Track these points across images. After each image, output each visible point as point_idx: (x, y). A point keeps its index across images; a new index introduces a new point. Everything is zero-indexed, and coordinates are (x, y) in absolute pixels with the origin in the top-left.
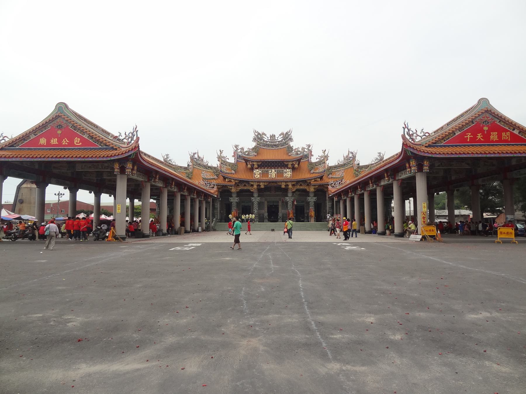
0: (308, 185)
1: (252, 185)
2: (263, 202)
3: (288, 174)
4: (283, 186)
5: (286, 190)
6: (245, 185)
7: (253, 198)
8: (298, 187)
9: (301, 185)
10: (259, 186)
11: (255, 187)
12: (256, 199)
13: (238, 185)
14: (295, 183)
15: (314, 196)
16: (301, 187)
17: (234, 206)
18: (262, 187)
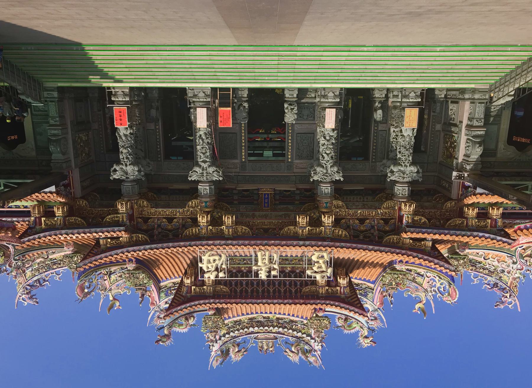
0: (146, 220)
1: (337, 222)
2: (300, 157)
3: (213, 262)
4: (228, 220)
5: (225, 197)
6: (362, 221)
7: (337, 177)
8: (178, 213)
9: (170, 220)
10: (316, 222)
11: (327, 220)
12: (326, 172)
13: (386, 221)
14: (187, 232)
15: (119, 181)
16: (168, 211)
17: (405, 155)
18: (302, 220)
